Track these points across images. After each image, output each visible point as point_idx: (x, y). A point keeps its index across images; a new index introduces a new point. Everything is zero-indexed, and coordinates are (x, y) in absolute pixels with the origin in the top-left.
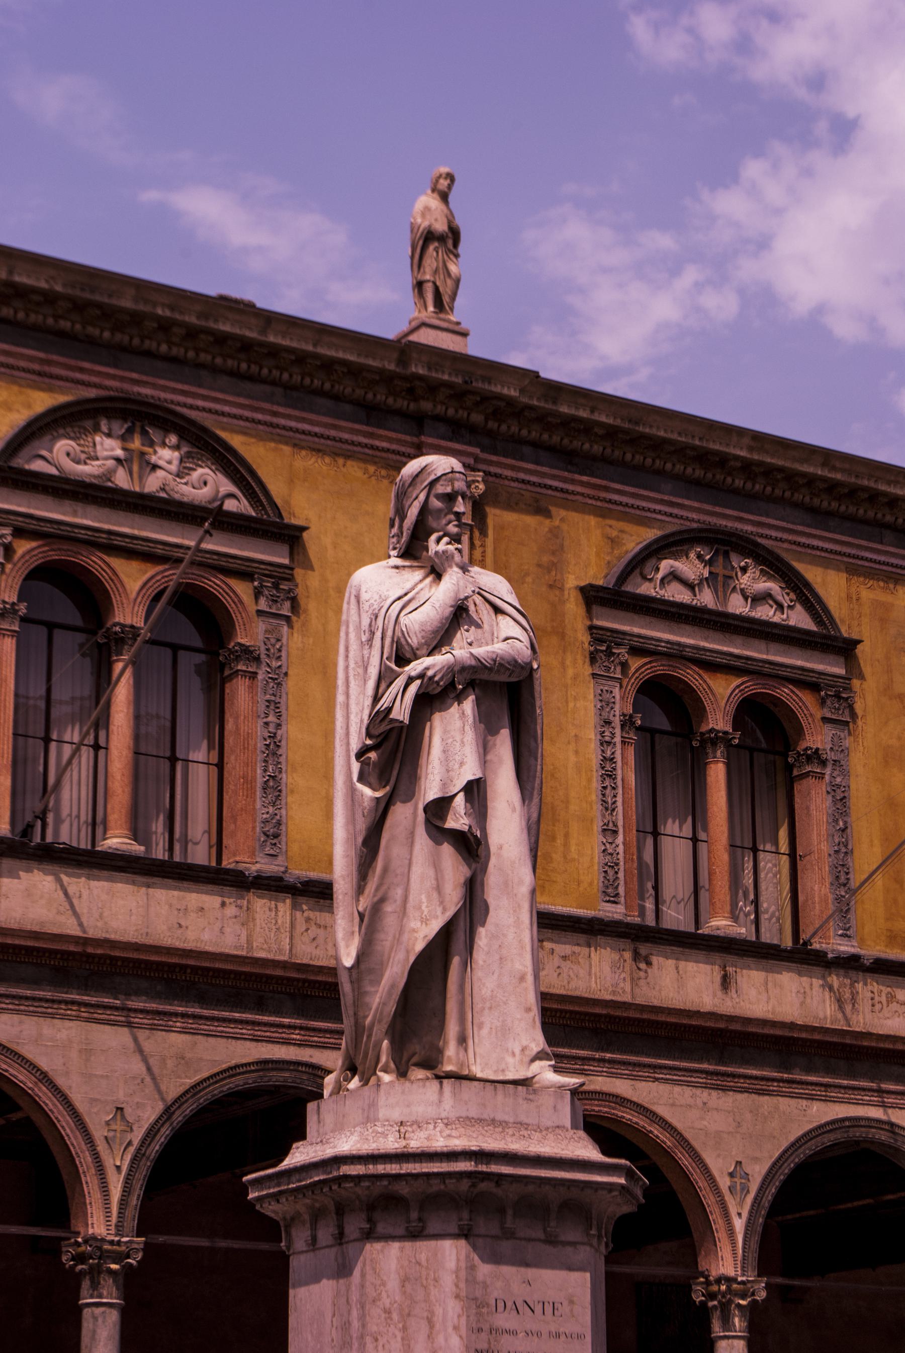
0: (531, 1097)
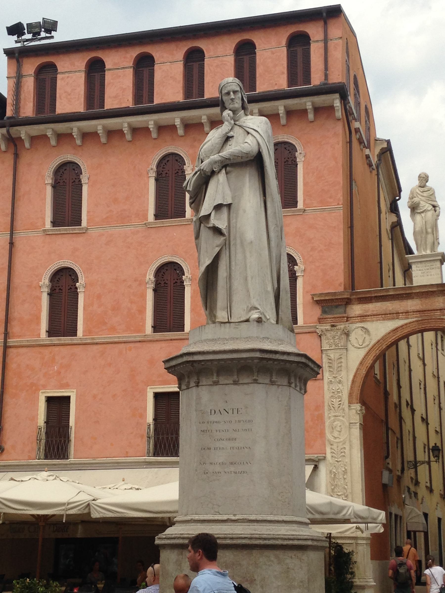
0: (237, 327)
